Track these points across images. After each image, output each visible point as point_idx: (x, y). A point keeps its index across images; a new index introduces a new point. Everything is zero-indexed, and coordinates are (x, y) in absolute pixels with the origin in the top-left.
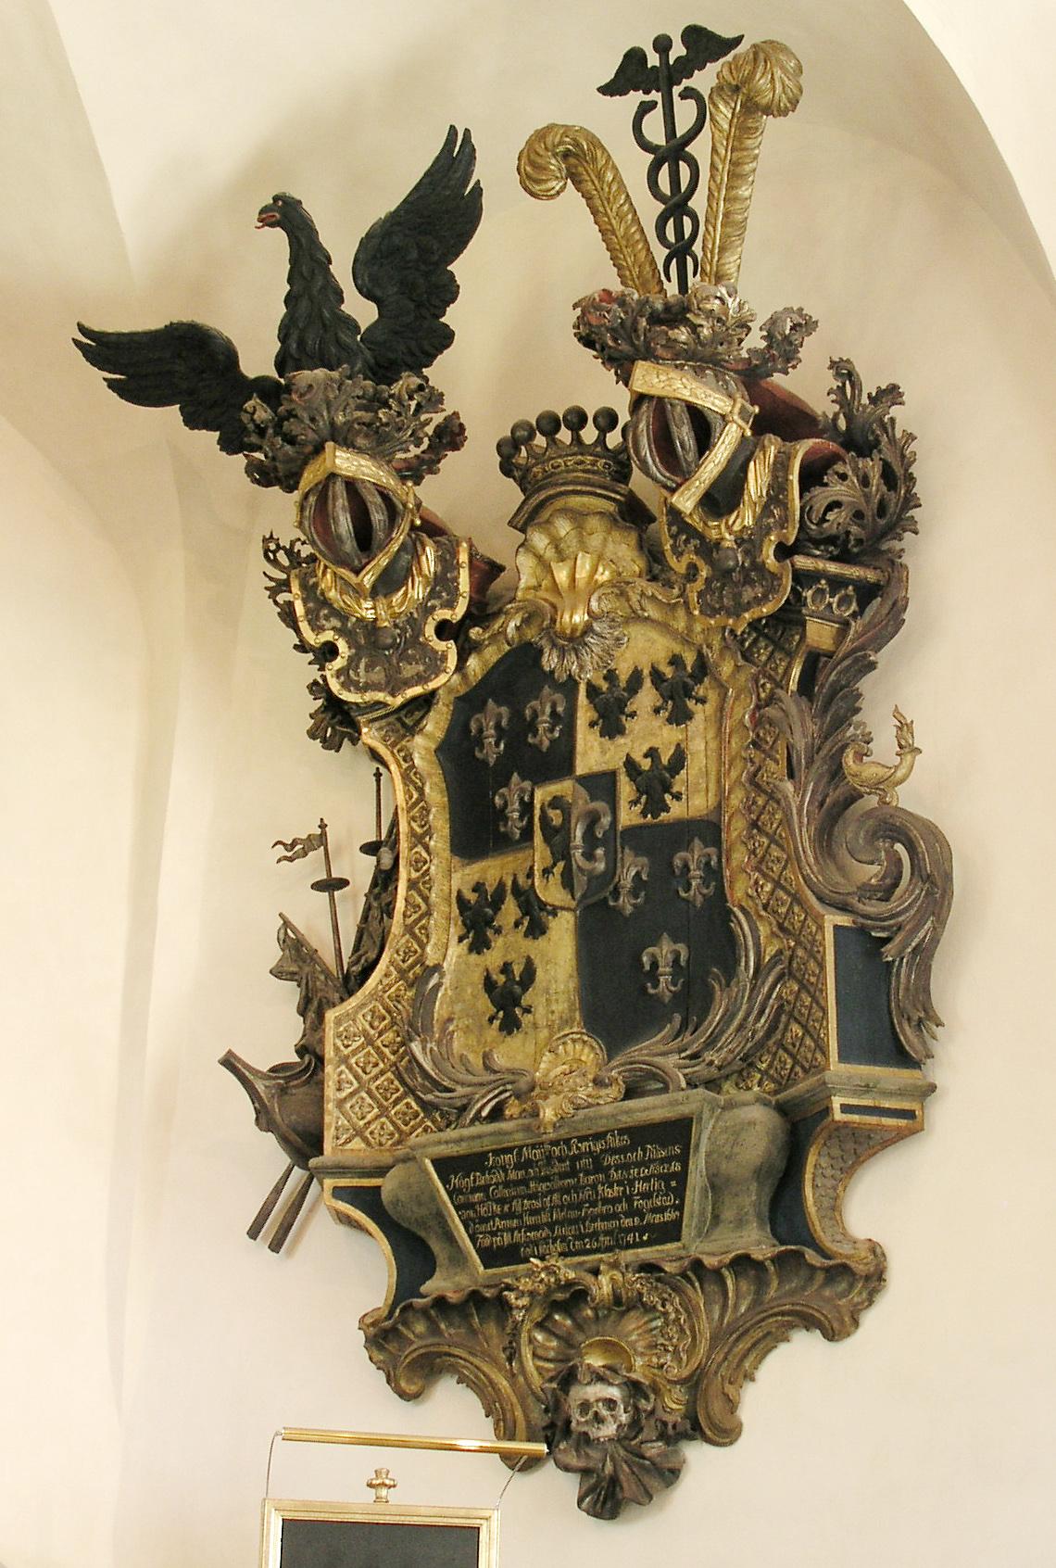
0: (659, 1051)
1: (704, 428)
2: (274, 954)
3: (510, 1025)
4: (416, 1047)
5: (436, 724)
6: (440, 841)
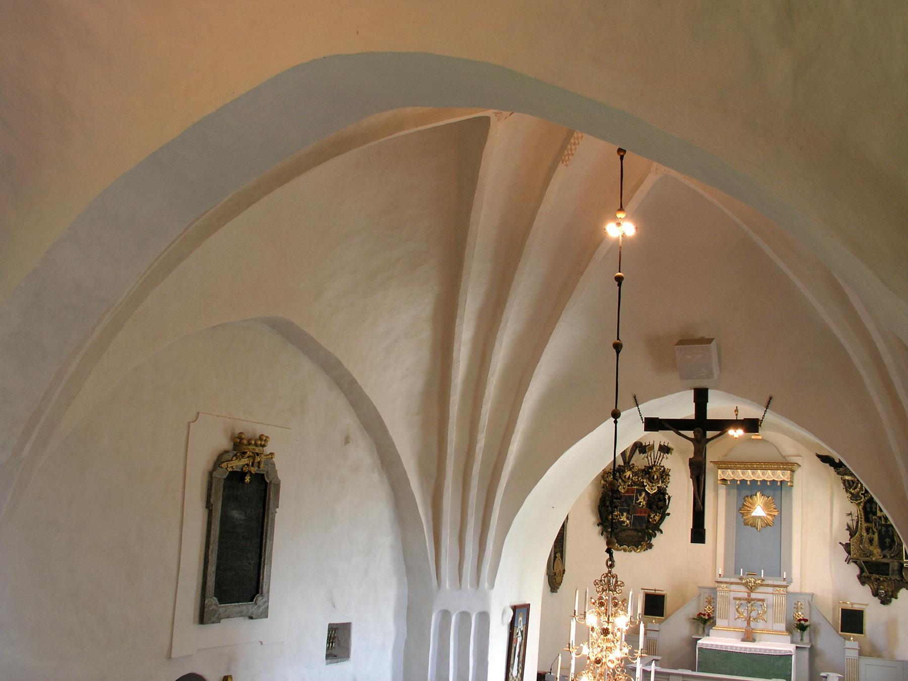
0: (886, 552)
2: (847, 527)
4: (861, 546)
5: (862, 504)
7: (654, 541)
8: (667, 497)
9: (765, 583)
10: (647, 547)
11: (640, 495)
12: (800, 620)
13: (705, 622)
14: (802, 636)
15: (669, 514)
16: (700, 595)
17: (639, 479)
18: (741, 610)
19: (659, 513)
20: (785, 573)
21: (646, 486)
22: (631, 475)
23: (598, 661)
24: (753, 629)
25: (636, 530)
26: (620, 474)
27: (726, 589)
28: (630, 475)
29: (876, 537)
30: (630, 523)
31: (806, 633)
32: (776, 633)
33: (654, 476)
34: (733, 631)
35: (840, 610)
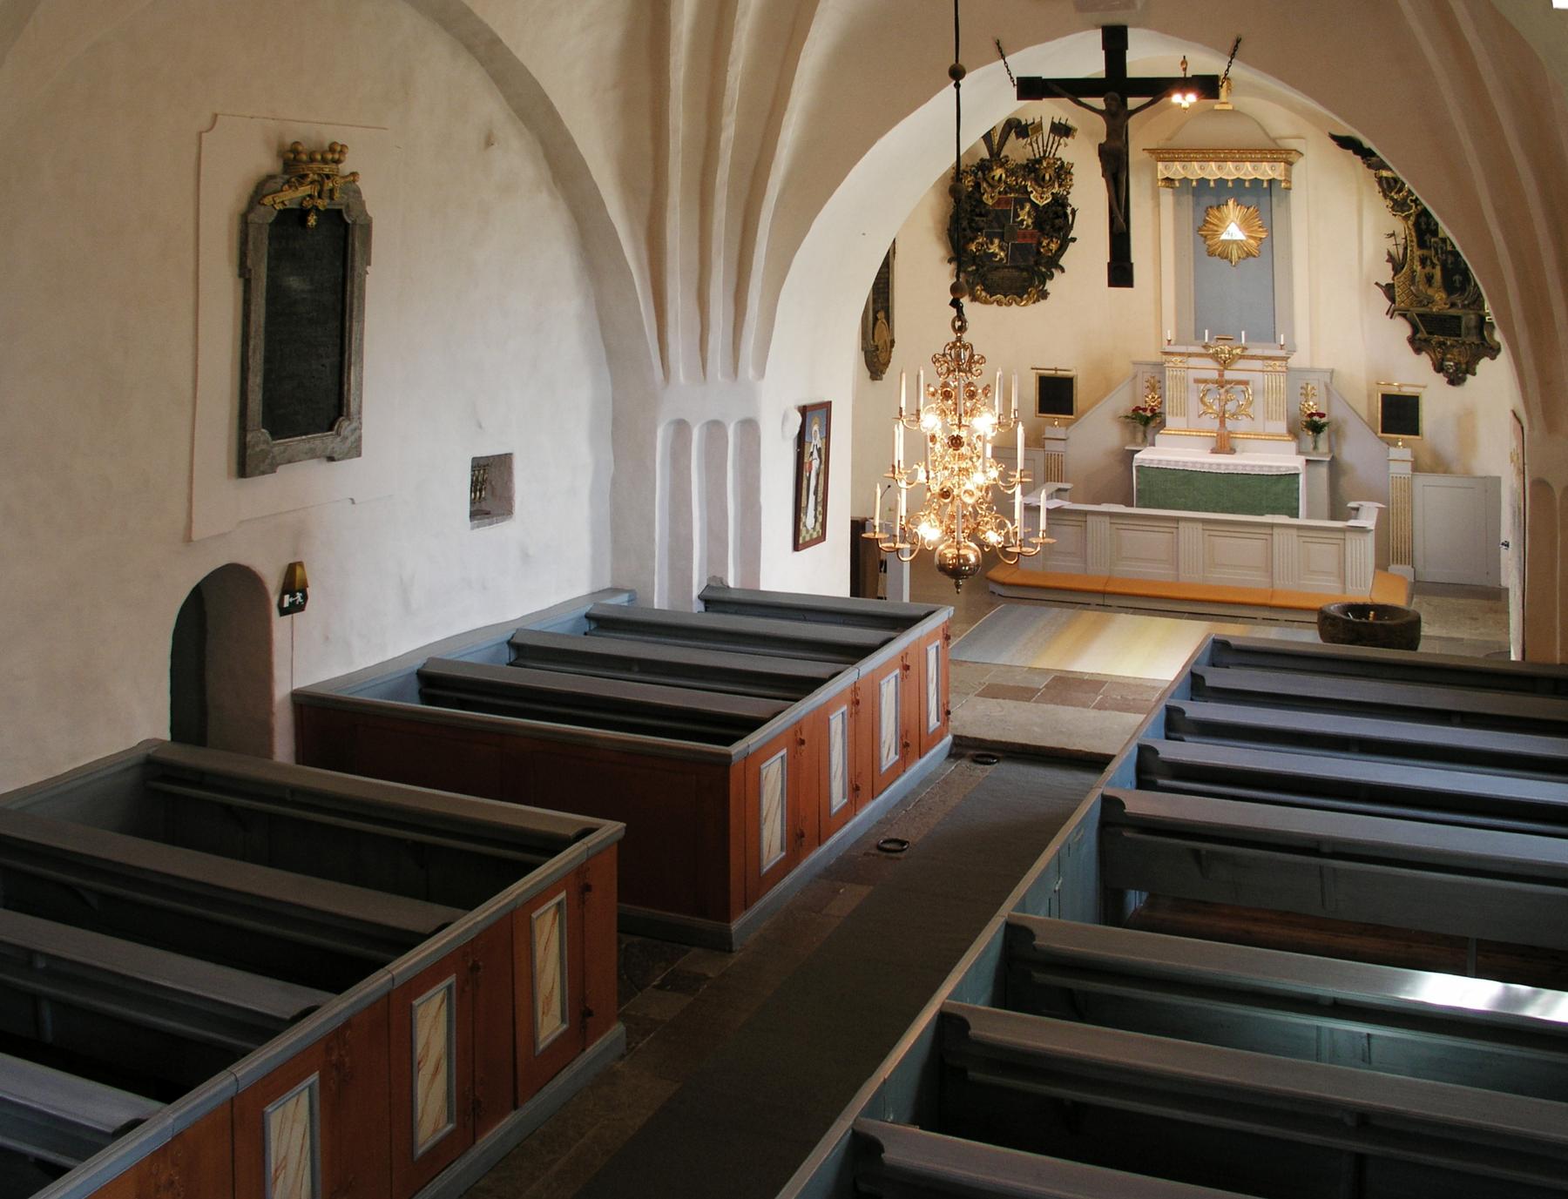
0: (1455, 297)
2: (1387, 257)
3: (1430, 286)
4: (1412, 288)
6: (1415, 244)
7: (1049, 286)
8: (1069, 210)
9: (1247, 353)
10: (1038, 296)
11: (1022, 209)
12: (1312, 415)
13: (1146, 421)
14: (1316, 442)
15: (1074, 240)
16: (1135, 377)
17: (1019, 181)
18: (1208, 399)
19: (1056, 238)
20: (1282, 336)
21: (1032, 192)
22: (1004, 176)
23: (945, 494)
24: (1230, 432)
25: (1017, 268)
26: (984, 174)
27: (1181, 365)
28: (1001, 175)
29: (1438, 272)
30: (1006, 255)
31: (1322, 435)
32: (1271, 438)
33: (1044, 176)
34: (1196, 436)
35: (1380, 395)
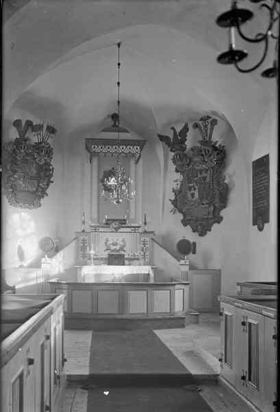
1: (208, 151)
8: (51, 167)
15: (52, 182)
